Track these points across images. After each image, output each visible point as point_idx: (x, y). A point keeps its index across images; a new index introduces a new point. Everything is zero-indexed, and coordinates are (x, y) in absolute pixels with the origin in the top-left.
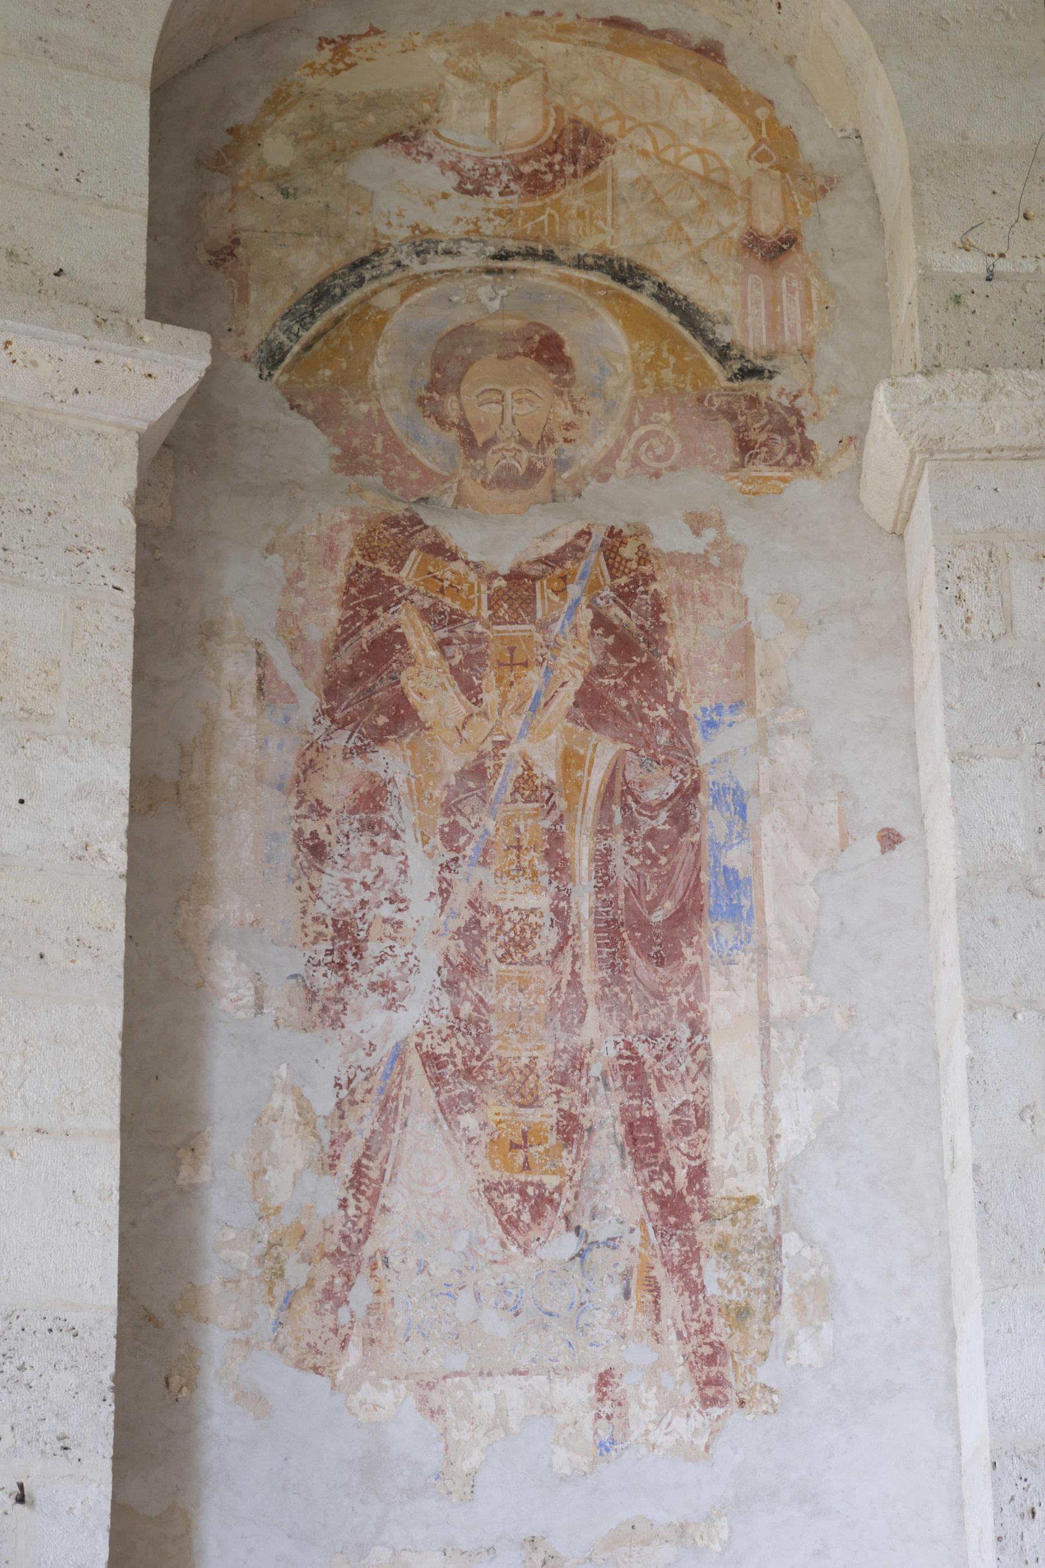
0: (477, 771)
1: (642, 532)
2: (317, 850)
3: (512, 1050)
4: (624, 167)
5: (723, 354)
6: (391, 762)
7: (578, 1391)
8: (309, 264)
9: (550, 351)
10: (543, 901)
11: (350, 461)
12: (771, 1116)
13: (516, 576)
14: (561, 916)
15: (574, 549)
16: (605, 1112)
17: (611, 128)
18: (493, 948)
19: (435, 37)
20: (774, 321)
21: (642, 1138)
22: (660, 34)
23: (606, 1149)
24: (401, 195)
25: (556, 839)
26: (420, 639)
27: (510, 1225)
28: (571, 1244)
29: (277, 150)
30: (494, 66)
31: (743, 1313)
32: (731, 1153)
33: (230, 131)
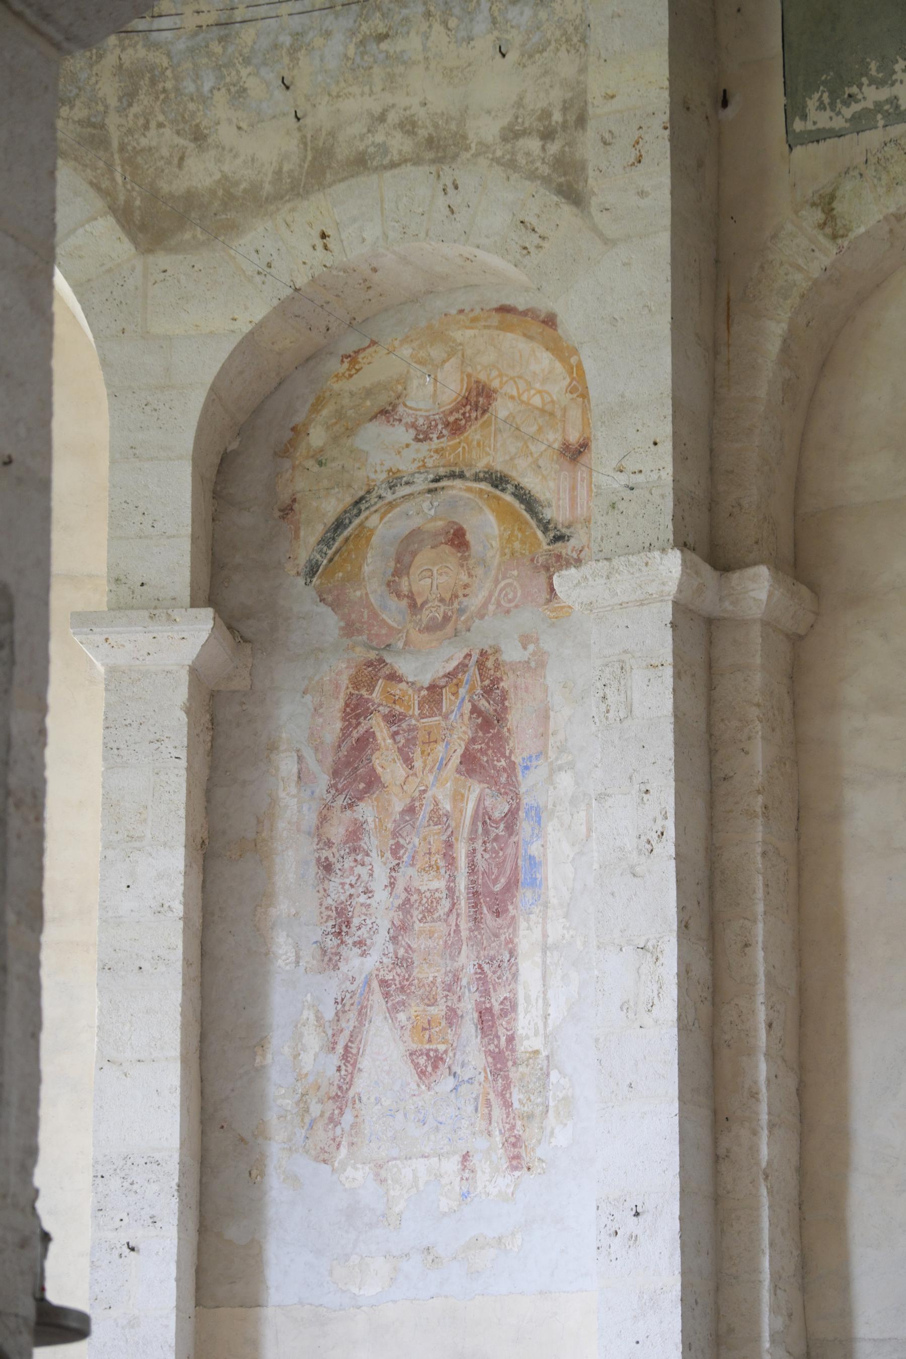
0: (411, 810)
1: (497, 651)
2: (328, 867)
3: (430, 973)
4: (502, 408)
5: (545, 526)
6: (366, 811)
7: (452, 1165)
8: (332, 507)
9: (458, 539)
10: (441, 884)
11: (350, 629)
12: (546, 1004)
13: (433, 688)
14: (451, 891)
15: (462, 667)
16: (468, 1006)
17: (495, 384)
18: (416, 914)
19: (406, 340)
20: (573, 499)
21: (486, 1020)
22: (525, 313)
23: (469, 1027)
24: (386, 449)
25: (449, 845)
26: (382, 733)
27: (422, 1073)
28: (451, 1082)
29: (317, 437)
30: (436, 352)
31: (530, 1116)
32: (527, 1027)
33: (293, 429)
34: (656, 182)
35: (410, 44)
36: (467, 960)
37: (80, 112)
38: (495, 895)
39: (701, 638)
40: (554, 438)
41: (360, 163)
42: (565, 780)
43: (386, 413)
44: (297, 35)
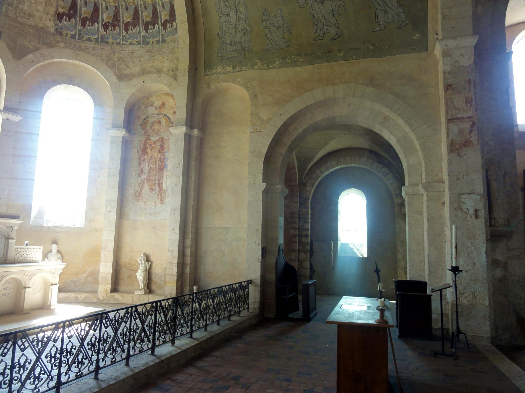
0: (151, 157)
2: (140, 164)
3: (152, 178)
4: (166, 106)
5: (171, 122)
6: (146, 157)
7: (154, 203)
8: (144, 117)
9: (160, 122)
11: (145, 133)
16: (157, 182)
21: (159, 185)
23: (157, 185)
24: (151, 110)
29: (143, 108)
30: (159, 98)
32: (164, 186)
34: (186, 78)
35: (156, 57)
36: (157, 177)
37: (112, 62)
38: (162, 168)
39: (188, 138)
40: (173, 111)
41: (149, 72)
42: (171, 154)
43: (152, 105)
44: (142, 55)
